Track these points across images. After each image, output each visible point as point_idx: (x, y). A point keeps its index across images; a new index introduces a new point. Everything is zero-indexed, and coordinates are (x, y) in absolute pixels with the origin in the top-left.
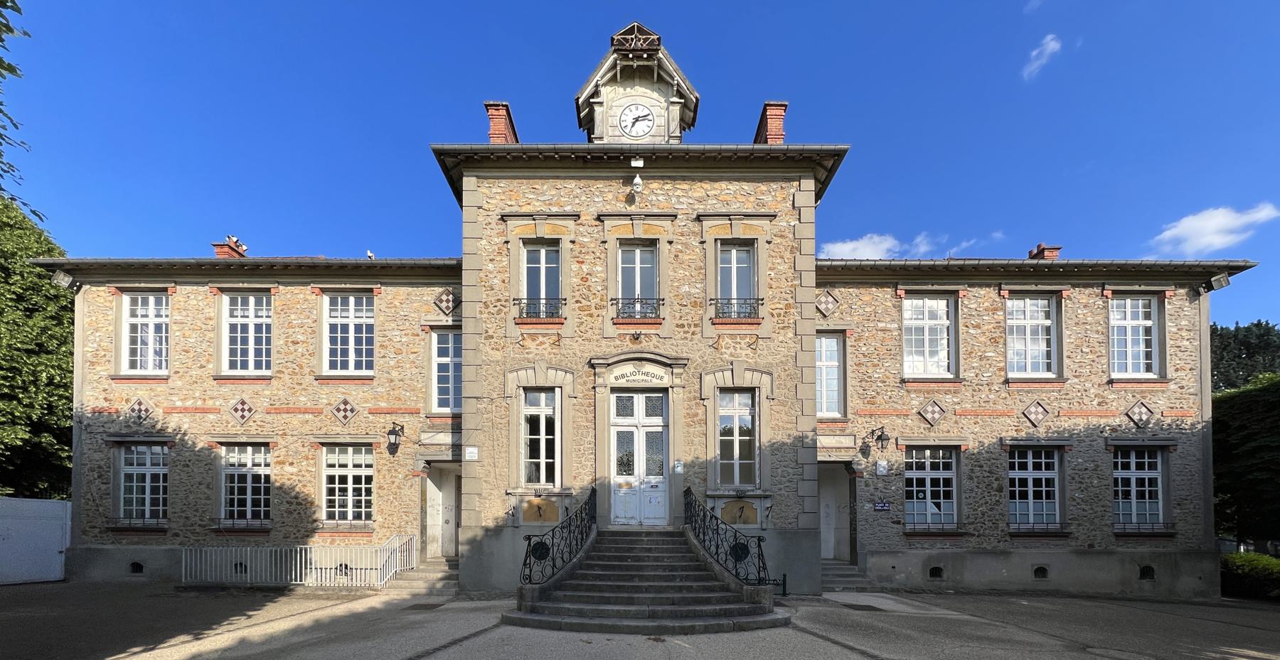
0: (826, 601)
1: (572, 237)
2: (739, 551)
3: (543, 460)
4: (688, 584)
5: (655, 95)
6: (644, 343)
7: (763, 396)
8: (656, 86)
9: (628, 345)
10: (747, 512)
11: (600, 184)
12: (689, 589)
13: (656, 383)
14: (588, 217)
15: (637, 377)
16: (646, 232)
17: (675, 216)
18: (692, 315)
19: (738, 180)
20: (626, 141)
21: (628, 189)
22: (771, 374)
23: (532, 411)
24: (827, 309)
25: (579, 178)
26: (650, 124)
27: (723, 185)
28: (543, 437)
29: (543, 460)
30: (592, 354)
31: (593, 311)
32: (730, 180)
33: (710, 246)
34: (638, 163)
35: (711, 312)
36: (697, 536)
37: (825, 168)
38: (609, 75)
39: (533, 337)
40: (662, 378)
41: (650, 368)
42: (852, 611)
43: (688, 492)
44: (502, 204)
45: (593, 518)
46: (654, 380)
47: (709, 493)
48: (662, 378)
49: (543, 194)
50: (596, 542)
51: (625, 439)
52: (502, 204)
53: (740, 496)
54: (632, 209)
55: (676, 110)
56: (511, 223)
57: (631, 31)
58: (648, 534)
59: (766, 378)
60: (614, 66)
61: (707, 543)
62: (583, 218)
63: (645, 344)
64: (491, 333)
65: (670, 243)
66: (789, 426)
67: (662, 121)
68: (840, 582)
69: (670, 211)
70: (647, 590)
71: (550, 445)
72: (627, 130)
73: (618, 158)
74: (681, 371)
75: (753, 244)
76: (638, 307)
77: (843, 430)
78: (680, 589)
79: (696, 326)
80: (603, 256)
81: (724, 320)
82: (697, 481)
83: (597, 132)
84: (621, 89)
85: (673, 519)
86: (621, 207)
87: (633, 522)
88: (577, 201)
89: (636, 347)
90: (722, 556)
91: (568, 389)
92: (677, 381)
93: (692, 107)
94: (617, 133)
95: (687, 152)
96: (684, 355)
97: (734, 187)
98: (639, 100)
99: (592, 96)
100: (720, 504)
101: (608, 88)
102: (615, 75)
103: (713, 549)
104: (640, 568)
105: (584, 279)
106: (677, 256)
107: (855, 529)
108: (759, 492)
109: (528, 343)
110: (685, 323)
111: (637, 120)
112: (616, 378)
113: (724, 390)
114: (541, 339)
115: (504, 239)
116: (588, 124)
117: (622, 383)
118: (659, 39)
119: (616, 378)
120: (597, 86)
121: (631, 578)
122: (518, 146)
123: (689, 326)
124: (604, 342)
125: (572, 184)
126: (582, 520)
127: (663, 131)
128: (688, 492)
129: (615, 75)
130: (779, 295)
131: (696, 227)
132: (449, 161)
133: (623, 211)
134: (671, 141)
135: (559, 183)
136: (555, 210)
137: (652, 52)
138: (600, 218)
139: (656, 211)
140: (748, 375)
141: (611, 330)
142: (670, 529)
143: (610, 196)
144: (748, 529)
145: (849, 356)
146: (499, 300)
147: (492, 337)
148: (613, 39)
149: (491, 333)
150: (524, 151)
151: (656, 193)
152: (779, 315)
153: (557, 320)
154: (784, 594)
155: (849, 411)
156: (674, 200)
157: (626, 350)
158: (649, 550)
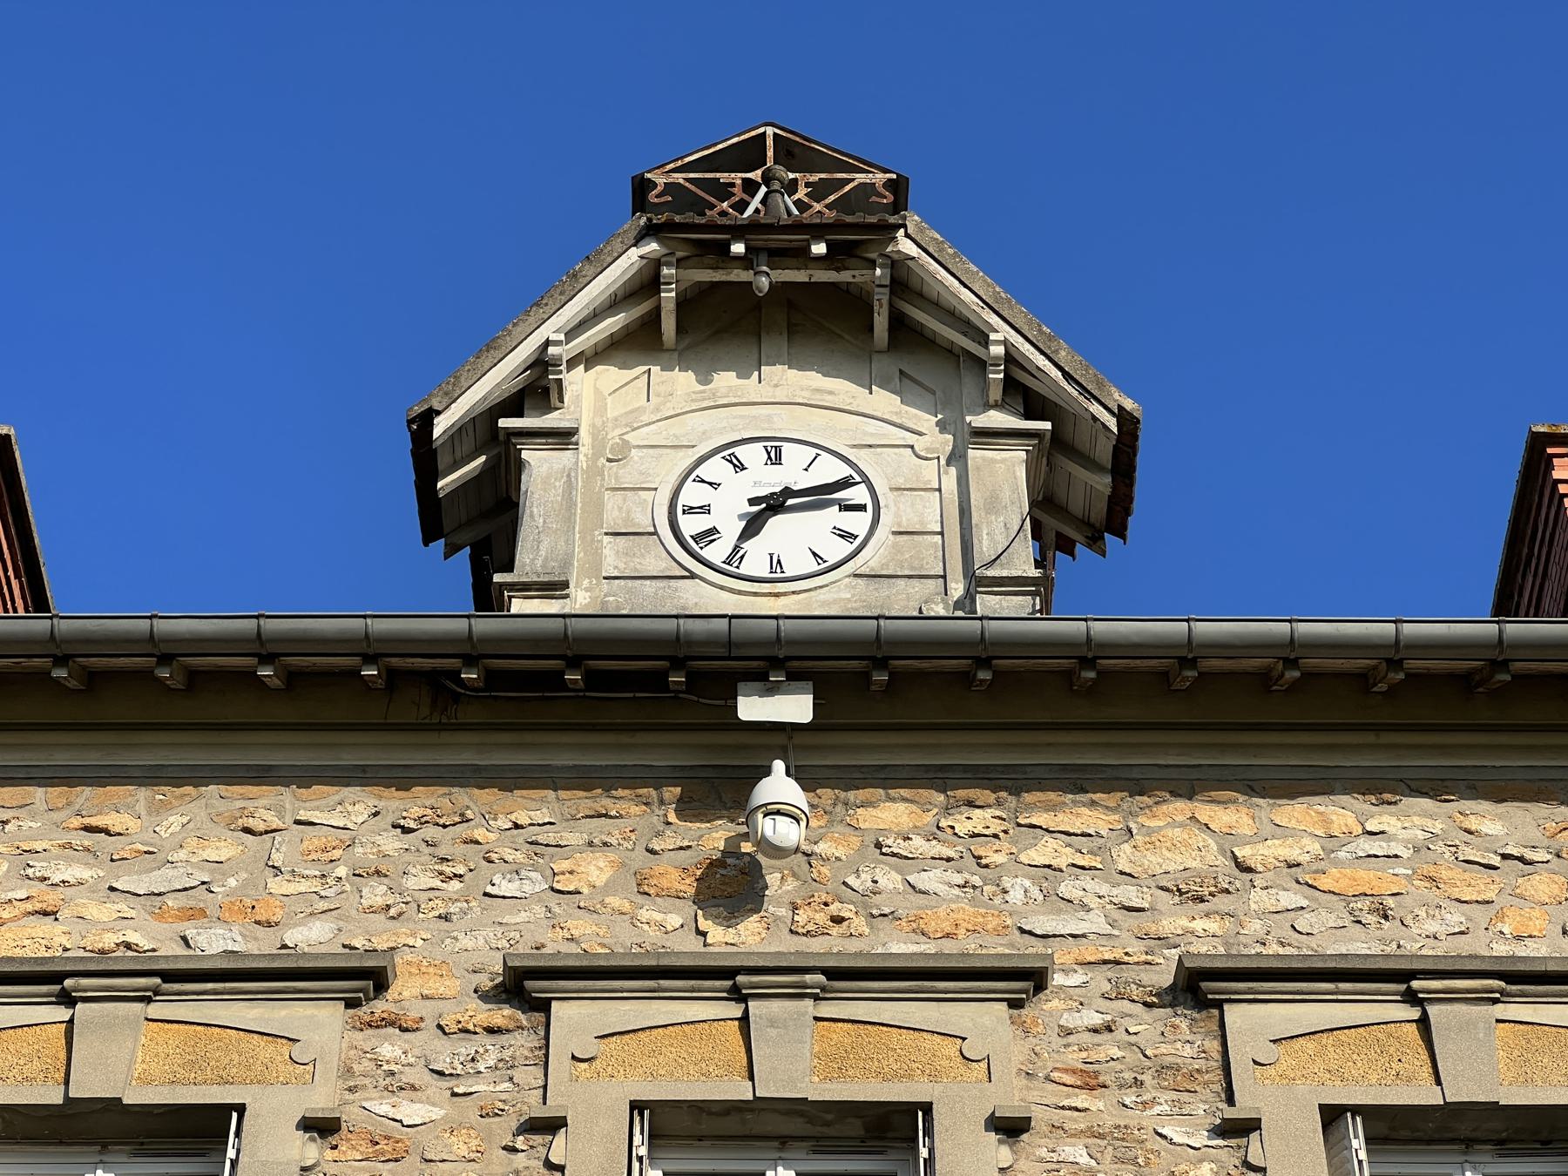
1: (320, 1101)
5: (884, 401)
11: (534, 809)
14: (441, 971)
16: (835, 1063)
17: (1036, 978)
19: (1435, 787)
20: (708, 599)
21: (715, 836)
25: (401, 779)
26: (858, 523)
27: (1342, 812)
32: (1381, 786)
34: (796, 707)
38: (612, 324)
54: (745, 938)
55: (1005, 474)
57: (749, 154)
60: (646, 284)
62: (404, 991)
65: (1010, 1128)
67: (928, 512)
72: (716, 553)
73: (657, 680)
83: (531, 558)
84: (682, 381)
86: (669, 928)
88: (376, 894)
95: (1088, 653)
97: (1409, 822)
98: (782, 422)
99: (514, 404)
101: (608, 375)
111: (774, 505)
116: (477, 516)
118: (898, 187)
120: (541, 364)
122: (40, 626)
125: (350, 810)
127: (928, 556)
129: (652, 322)
131: (1182, 1039)
133: (685, 948)
134: (987, 603)
135: (267, 805)
136: (215, 942)
137: (861, 231)
138: (524, 988)
139: (900, 946)
143: (595, 870)
148: (641, 187)
150: (61, 651)
151: (888, 862)
156: (1019, 889)
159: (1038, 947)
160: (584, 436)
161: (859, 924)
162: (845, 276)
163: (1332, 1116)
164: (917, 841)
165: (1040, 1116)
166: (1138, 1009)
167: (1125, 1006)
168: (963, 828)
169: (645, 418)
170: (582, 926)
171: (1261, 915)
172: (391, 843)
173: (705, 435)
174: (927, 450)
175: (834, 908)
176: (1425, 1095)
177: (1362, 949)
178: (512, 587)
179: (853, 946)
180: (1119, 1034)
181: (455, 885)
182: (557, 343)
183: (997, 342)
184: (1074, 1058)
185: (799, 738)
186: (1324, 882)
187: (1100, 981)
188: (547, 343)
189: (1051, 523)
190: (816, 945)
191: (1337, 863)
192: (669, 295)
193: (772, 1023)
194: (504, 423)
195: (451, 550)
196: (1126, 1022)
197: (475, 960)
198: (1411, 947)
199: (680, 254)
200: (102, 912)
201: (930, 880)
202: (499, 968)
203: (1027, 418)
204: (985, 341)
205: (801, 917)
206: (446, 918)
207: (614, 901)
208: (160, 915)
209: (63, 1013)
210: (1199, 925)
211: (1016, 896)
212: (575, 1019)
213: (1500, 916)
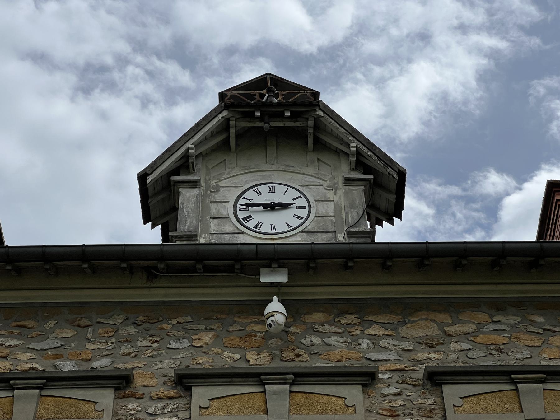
8: (313, 156)
26: (304, 213)
34: (281, 278)
49: (43, 336)
69: (357, 365)
88: (126, 348)
93: (393, 185)
94: (228, 228)
99: (176, 171)
143: (207, 338)
159: (372, 364)
160: (203, 183)
161: (306, 357)
162: (297, 124)
164: (327, 326)
166: (410, 387)
167: (405, 386)
168: (343, 321)
169: (224, 177)
170: (202, 359)
171: (455, 352)
172: (132, 330)
173: (246, 182)
174: (329, 187)
175: (297, 351)
177: (492, 363)
178: (176, 236)
179: (303, 365)
180: (404, 396)
181: (156, 345)
182: (192, 149)
183: (353, 147)
184: (386, 405)
185: (284, 290)
186: (478, 340)
187: (396, 377)
188: (188, 149)
191: (483, 333)
192: (232, 131)
193: (275, 393)
194: (173, 178)
196: (406, 392)
199: (237, 117)
201: (333, 340)
202: (172, 375)
203: (364, 174)
204: (349, 146)
205: (284, 355)
206: (152, 357)
207: (216, 350)
209: (9, 394)
210: (433, 356)
211: (364, 346)
212: (201, 394)
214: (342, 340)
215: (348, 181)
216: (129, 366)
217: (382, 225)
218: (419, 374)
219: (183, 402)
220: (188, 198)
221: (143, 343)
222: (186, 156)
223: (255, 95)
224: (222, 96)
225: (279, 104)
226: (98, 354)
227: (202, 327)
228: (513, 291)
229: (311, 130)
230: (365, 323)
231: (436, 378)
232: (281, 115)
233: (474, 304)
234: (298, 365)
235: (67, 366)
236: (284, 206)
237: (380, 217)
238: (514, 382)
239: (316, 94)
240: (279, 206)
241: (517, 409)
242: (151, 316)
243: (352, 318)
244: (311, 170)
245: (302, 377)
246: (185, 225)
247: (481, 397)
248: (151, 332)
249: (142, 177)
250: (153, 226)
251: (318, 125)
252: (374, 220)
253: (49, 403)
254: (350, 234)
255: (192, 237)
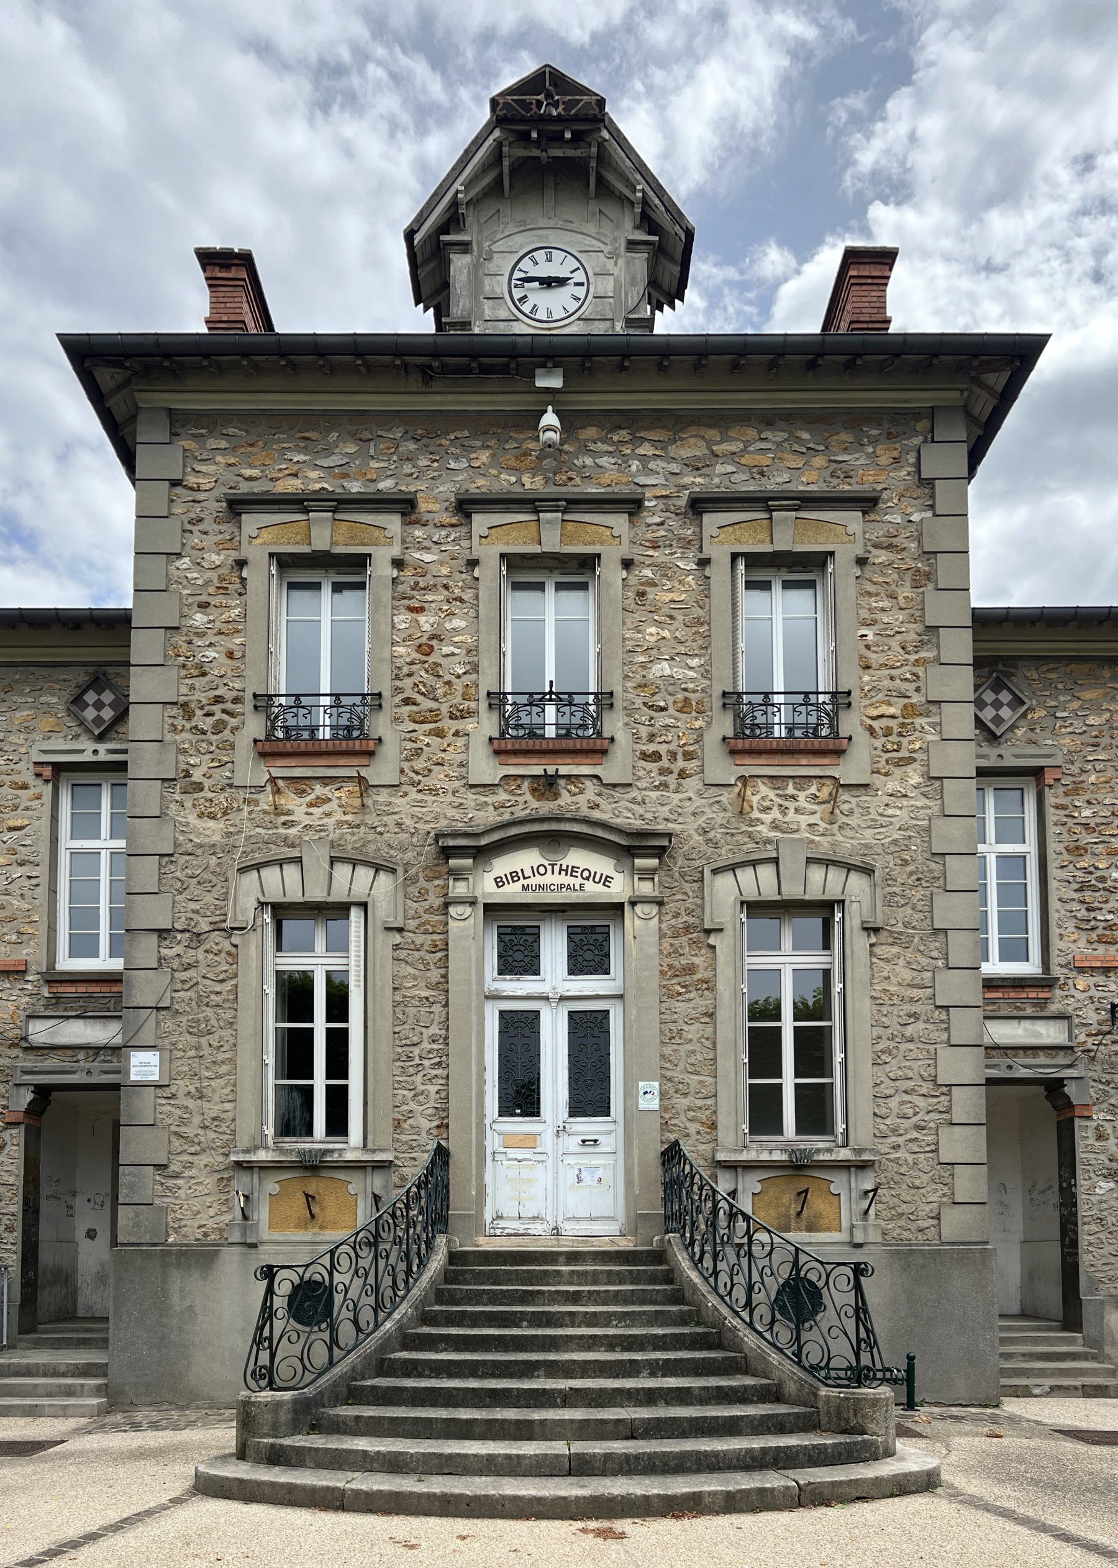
0: (1013, 1420)
2: (799, 1299)
3: (320, 1082)
4: (672, 1382)
6: (565, 799)
7: (854, 923)
8: (594, 206)
9: (527, 804)
10: (817, 1203)
12: (681, 1396)
13: (593, 891)
14: (434, 500)
15: (549, 879)
18: (679, 729)
22: (868, 871)
23: (293, 963)
24: (998, 720)
26: (581, 292)
28: (320, 1025)
29: (320, 1082)
30: (443, 824)
31: (447, 724)
33: (719, 572)
35: (725, 725)
36: (697, 1263)
37: (990, 389)
39: (300, 784)
40: (606, 880)
41: (578, 858)
42: (1082, 1448)
43: (672, 1154)
44: (229, 477)
45: (439, 1221)
46: (590, 886)
47: (721, 1156)
48: (606, 880)
49: (328, 452)
50: (449, 1277)
51: (519, 1030)
52: (229, 477)
53: (798, 1167)
56: (251, 522)
58: (574, 1257)
59: (856, 881)
61: (724, 1278)
63: (565, 800)
64: (197, 776)
66: (916, 993)
68: (1043, 1373)
69: (623, 490)
70: (570, 1399)
71: (338, 1042)
74: (654, 862)
75: (824, 565)
76: (551, 711)
77: (1043, 1003)
78: (649, 1397)
79: (688, 756)
80: (468, 595)
81: (755, 743)
82: (693, 1128)
85: (636, 1222)
87: (537, 1228)
88: (407, 468)
89: (545, 807)
90: (763, 1311)
91: (384, 909)
92: (646, 888)
94: (503, 314)
96: (661, 827)
100: (750, 1184)
102: (498, 181)
103: (740, 1294)
104: (552, 1343)
105: (426, 650)
106: (642, 594)
107: (1075, 1243)
108: (844, 1154)
109: (291, 801)
110: (663, 749)
112: (499, 882)
113: (755, 908)
114: (319, 790)
115: (234, 555)
117: (512, 892)
119: (499, 882)
121: (528, 1370)
123: (673, 755)
124: (471, 797)
126: (411, 1224)
128: (672, 1154)
130: (886, 683)
132: (107, 377)
140: (817, 874)
141: (486, 769)
142: (626, 1244)
143: (484, 457)
144: (824, 1243)
145: (1052, 830)
146: (218, 700)
147: (199, 787)
149: (197, 776)
152: (888, 732)
153: (357, 745)
154: (911, 1404)
155: (1055, 960)
156: (635, 465)
157: (521, 814)
158: (575, 1298)
160: (475, 247)
161: (578, 480)
163: (735, 557)
164: (599, 444)
165: (637, 558)
166: (673, 515)
167: (668, 514)
168: (616, 438)
169: (499, 236)
170: (481, 482)
171: (719, 475)
172: (412, 446)
173: (522, 246)
174: (610, 253)
176: (766, 548)
177: (752, 488)
179: (576, 490)
180: (666, 526)
181: (436, 464)
182: (461, 192)
183: (639, 191)
184: (649, 536)
185: (559, 397)
186: (743, 461)
188: (457, 192)
189: (656, 295)
190: (563, 489)
191: (750, 453)
192: (506, 163)
193: (548, 522)
194: (444, 238)
195: (426, 309)
196: (668, 521)
197: (445, 496)
198: (770, 488)
199: (511, 139)
200: (314, 475)
201: (604, 461)
202: (453, 499)
203: (650, 234)
206: (433, 478)
207: (494, 472)
208: (334, 477)
209: (304, 517)
210: (698, 480)
211: (634, 468)
212: (481, 522)
213: (802, 474)
214: (613, 461)
215: (632, 245)
216: (412, 489)
217: (662, 311)
218: (683, 502)
219: (464, 529)
220: (460, 264)
221: (423, 462)
222: (454, 204)
223: (531, 104)
224: (494, 102)
225: (559, 119)
226: (382, 474)
227: (478, 443)
228: (785, 400)
229: (593, 164)
230: (636, 441)
231: (699, 506)
232: (559, 138)
233: (743, 417)
234: (570, 490)
235: (355, 487)
236: (561, 282)
237: (663, 300)
238: (770, 510)
239: (601, 102)
240: (554, 280)
241: (768, 539)
242: (430, 428)
243: (624, 435)
244: (591, 228)
245: (575, 503)
246: (458, 310)
247: (737, 527)
248: (431, 449)
249: (409, 235)
250: (426, 309)
251: (603, 156)
252: (655, 304)
253: (343, 528)
254: (629, 322)
255: (466, 324)
